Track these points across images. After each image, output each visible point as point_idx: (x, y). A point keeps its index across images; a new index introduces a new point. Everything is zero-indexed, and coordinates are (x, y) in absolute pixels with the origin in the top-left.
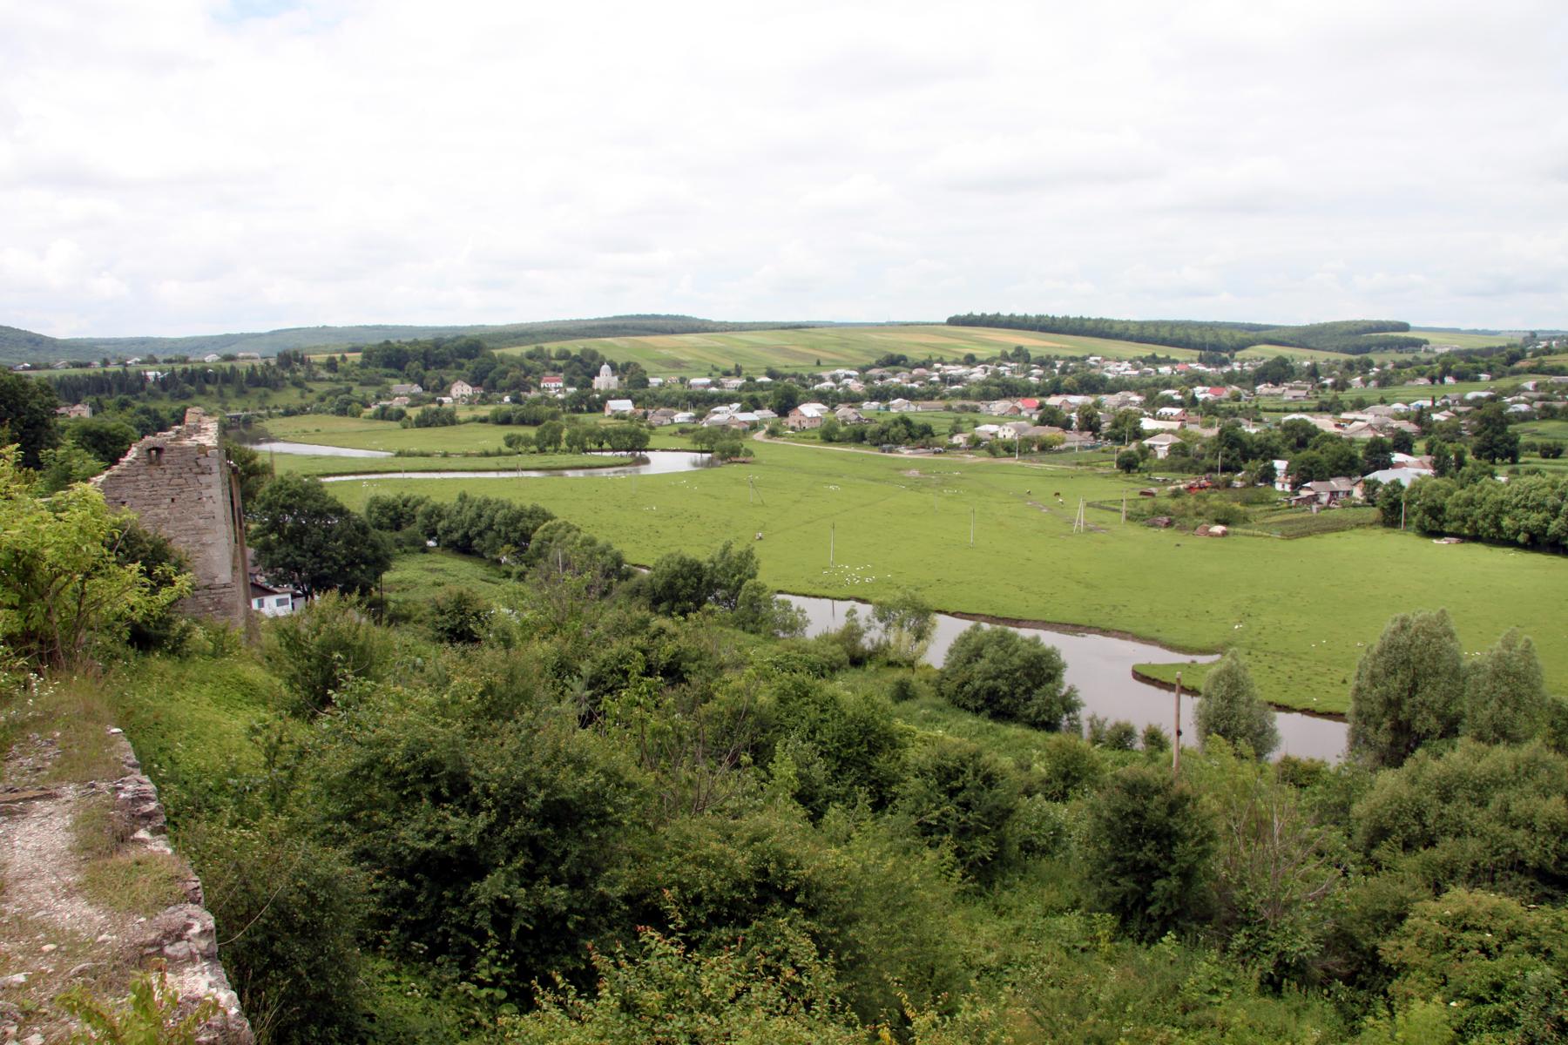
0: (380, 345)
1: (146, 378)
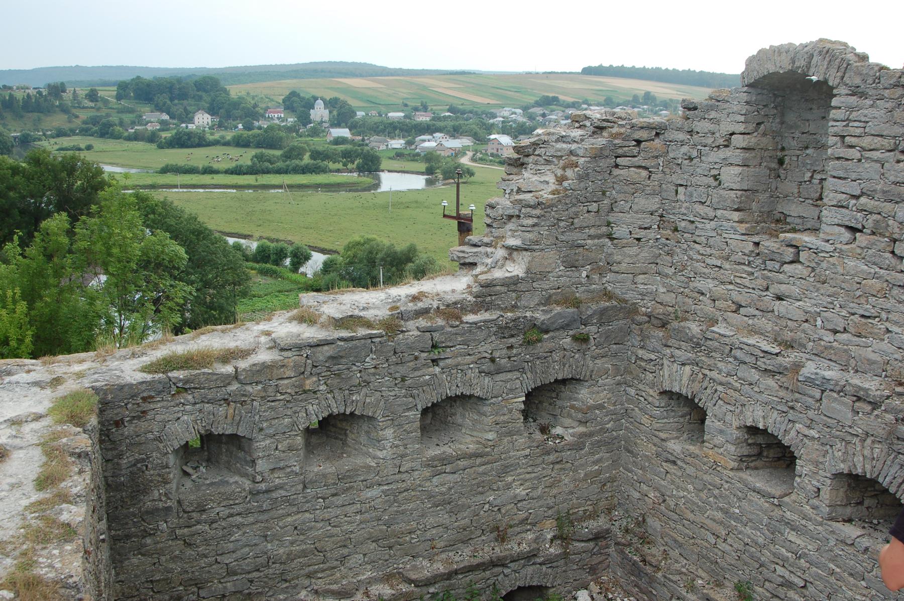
0: (133, 80)
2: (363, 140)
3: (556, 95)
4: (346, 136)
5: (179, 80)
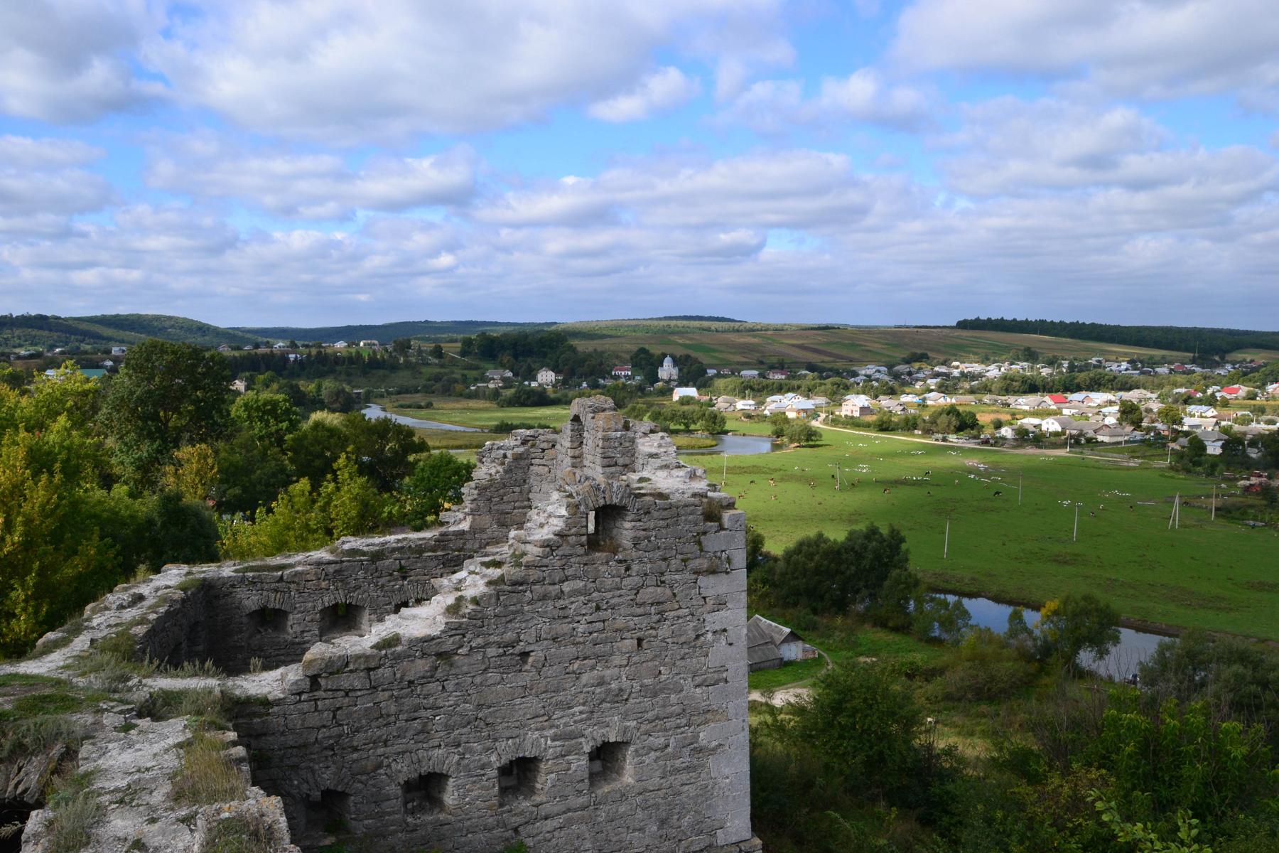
1: (288, 359)
2: (711, 400)
3: (926, 352)
4: (691, 395)
5: (526, 336)
